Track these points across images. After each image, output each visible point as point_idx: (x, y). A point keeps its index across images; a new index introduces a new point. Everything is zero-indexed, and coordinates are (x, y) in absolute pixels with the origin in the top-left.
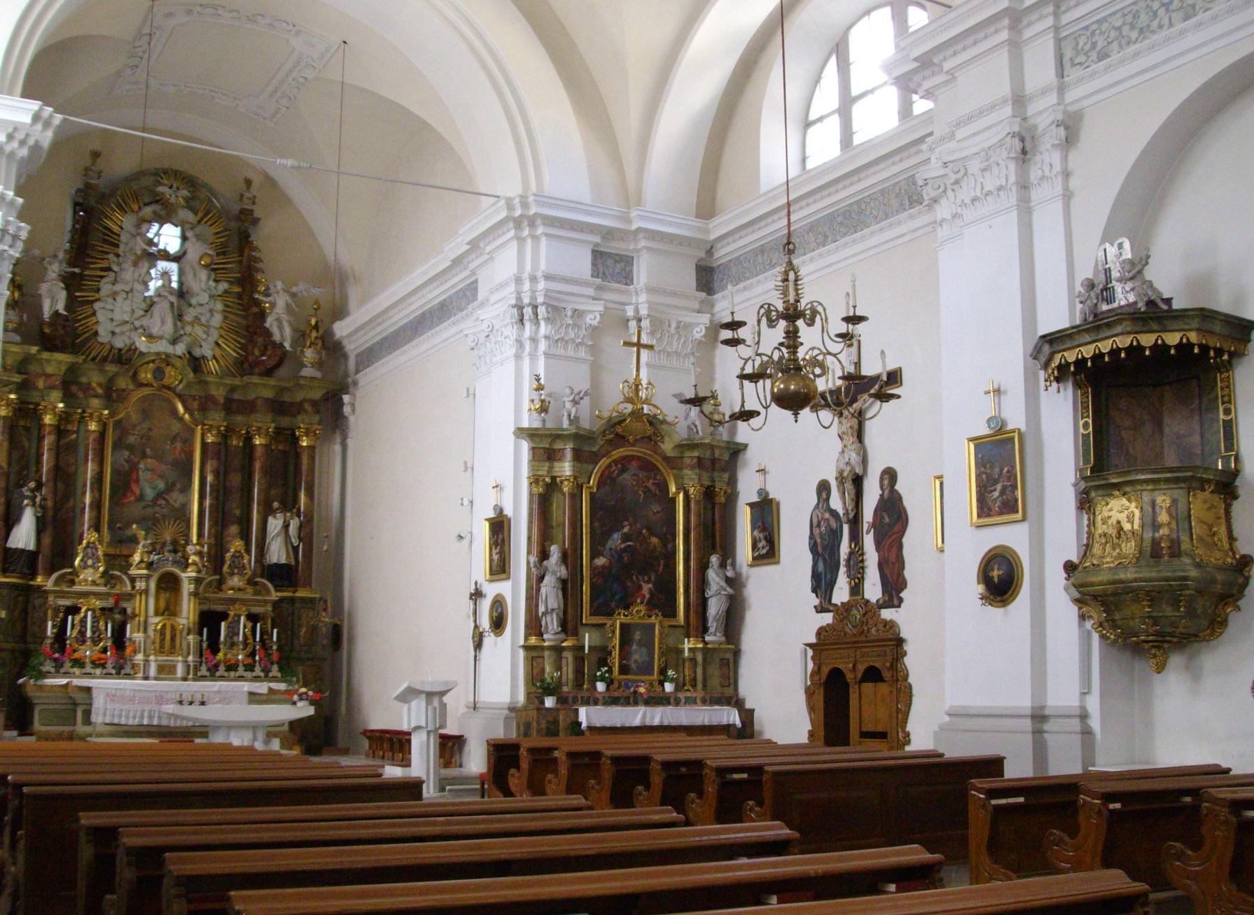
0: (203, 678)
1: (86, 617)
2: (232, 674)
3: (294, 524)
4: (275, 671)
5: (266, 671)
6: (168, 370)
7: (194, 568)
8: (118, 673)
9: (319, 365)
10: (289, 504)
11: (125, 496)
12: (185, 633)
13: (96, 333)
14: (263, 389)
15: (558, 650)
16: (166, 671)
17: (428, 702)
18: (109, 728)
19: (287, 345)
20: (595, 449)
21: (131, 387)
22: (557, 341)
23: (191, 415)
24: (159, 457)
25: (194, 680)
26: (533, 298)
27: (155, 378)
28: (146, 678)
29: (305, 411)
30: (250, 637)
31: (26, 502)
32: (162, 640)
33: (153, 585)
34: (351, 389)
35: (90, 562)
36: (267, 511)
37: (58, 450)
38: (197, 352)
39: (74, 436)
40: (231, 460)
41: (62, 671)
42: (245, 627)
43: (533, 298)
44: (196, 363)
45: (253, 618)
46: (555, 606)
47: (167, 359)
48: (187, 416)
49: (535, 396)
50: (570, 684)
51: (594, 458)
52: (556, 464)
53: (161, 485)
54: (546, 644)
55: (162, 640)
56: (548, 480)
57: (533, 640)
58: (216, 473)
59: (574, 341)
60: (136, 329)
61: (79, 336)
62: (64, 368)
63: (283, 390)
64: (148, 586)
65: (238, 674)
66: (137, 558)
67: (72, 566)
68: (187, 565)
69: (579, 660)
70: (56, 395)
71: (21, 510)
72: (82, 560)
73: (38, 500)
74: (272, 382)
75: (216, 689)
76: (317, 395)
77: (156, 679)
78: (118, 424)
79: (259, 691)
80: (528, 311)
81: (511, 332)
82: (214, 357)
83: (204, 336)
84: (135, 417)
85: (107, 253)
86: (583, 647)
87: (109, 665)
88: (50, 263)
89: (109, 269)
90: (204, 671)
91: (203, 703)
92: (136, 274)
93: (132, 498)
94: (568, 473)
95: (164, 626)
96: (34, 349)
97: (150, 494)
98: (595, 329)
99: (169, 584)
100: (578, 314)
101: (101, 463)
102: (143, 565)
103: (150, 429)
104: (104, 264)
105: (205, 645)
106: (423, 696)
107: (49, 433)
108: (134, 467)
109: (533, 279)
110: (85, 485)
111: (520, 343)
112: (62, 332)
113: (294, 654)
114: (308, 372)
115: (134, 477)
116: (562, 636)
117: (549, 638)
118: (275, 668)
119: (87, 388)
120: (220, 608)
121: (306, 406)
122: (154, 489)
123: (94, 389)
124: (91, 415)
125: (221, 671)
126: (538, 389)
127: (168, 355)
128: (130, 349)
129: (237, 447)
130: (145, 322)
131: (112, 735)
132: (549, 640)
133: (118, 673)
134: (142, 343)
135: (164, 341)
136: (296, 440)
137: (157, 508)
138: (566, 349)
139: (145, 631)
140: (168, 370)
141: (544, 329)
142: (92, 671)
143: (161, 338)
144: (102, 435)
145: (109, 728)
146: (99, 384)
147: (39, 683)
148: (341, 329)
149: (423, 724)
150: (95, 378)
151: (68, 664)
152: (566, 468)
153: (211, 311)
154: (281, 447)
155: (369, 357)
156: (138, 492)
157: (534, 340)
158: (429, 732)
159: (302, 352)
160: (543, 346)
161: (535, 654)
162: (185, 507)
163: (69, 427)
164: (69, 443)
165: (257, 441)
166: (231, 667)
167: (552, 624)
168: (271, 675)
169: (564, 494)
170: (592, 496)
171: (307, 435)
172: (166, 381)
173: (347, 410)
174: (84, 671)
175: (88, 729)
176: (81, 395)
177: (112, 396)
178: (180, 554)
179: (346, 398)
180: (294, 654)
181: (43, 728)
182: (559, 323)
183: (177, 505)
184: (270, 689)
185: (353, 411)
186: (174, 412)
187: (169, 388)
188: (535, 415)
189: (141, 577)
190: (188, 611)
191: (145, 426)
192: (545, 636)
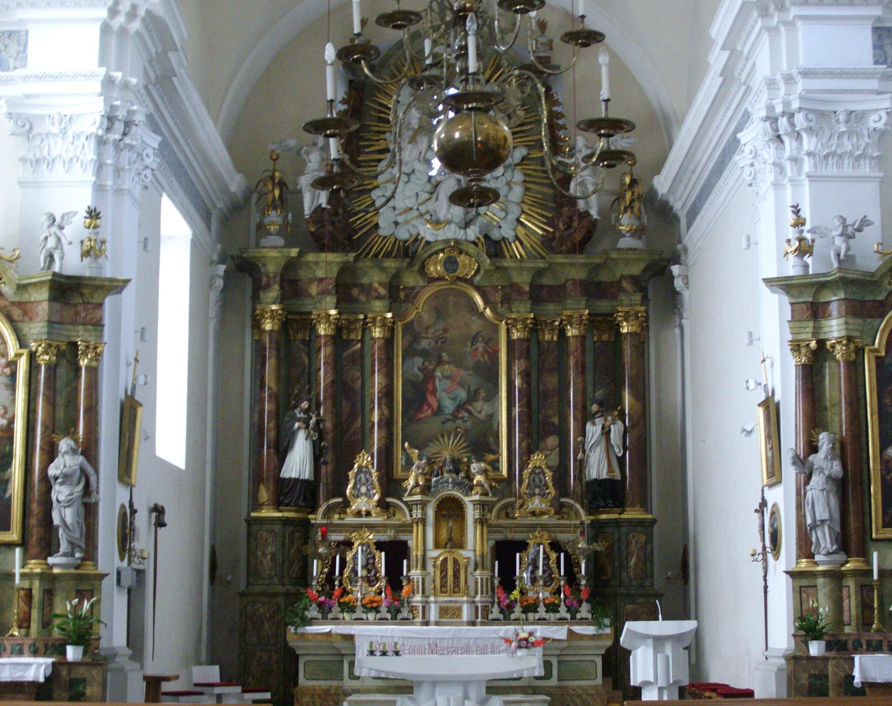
0: (496, 621)
1: (357, 553)
2: (531, 616)
3: (616, 430)
4: (585, 611)
5: (573, 611)
6: (462, 259)
7: (479, 489)
8: (394, 618)
9: (638, 232)
10: (611, 405)
11: (419, 410)
12: (471, 568)
13: (377, 226)
14: (572, 268)
15: (836, 576)
16: (449, 614)
17: (657, 650)
18: (379, 683)
19: (594, 213)
20: (881, 297)
21: (421, 283)
22: (826, 156)
23: (493, 310)
24: (458, 362)
25: (483, 624)
26: (787, 104)
27: (447, 270)
28: (427, 623)
29: (625, 291)
30: (555, 570)
31: (297, 425)
32: (444, 577)
33: (431, 512)
34: (683, 258)
35: (363, 489)
36: (585, 418)
37: (337, 364)
38: (495, 235)
39: (359, 345)
40: (540, 357)
41: (330, 616)
42: (547, 558)
43: (787, 104)
44: (495, 248)
45: (556, 546)
46: (826, 516)
47: (457, 246)
48: (488, 311)
49: (792, 233)
50: (853, 623)
51: (879, 310)
52: (824, 322)
53: (462, 394)
54: (820, 568)
55: (444, 577)
56: (813, 344)
57: (804, 565)
58: (526, 375)
59: (851, 154)
60: (421, 215)
61: (356, 232)
62: (336, 269)
63: (597, 267)
64: (424, 514)
65: (537, 616)
66: (411, 481)
67: (343, 495)
68: (471, 488)
69: (865, 589)
70: (331, 300)
71: (293, 435)
72: (354, 487)
73: (312, 422)
74: (580, 259)
75: (502, 634)
76: (636, 270)
77: (437, 624)
78: (408, 328)
79: (556, 636)
80: (783, 122)
81: (769, 153)
82: (517, 238)
83: (503, 214)
85: (384, 133)
86: (872, 571)
87: (383, 609)
88: (308, 153)
89: (386, 150)
90: (495, 613)
91: (397, 653)
92: (415, 154)
93: (429, 412)
94: (836, 334)
95: (446, 559)
96: (294, 252)
97: (449, 406)
98: (883, 133)
99: (451, 510)
100: (855, 117)
101: (389, 375)
102: (418, 490)
103: (446, 330)
104: (382, 145)
105: (496, 582)
106: (650, 641)
107: (325, 345)
108: (429, 376)
109: (789, 79)
110: (373, 401)
111: (779, 167)
112: (330, 228)
113: (622, 590)
114: (626, 242)
115: (430, 387)
116: (841, 557)
117: (822, 562)
118: (585, 607)
119: (367, 290)
120: (519, 537)
121: (625, 284)
122: (454, 399)
123: (376, 290)
124: (374, 319)
125: (517, 612)
126: (795, 225)
127: (457, 242)
128: (416, 239)
129: (550, 342)
130: (430, 206)
131: (380, 690)
132: (823, 563)
133: (394, 618)
134: (427, 232)
135: (453, 226)
136: (618, 326)
137: (459, 422)
138: (840, 166)
139: (424, 567)
140: (462, 259)
141: (808, 143)
142: (364, 616)
143: (449, 222)
144: (389, 342)
145: (379, 683)
146: (381, 284)
147: (300, 630)
148: (662, 184)
149: (652, 679)
150: (375, 278)
151: (336, 609)
152: (835, 328)
153: (508, 184)
154: (605, 337)
155: (693, 214)
156: (435, 405)
157: (795, 160)
158: (661, 690)
159: (618, 220)
160: (807, 165)
161: (805, 582)
162: (492, 417)
163: (353, 336)
164: (354, 352)
165: (571, 332)
166: (530, 608)
167: (824, 539)
168: (578, 616)
169: (838, 362)
170: (880, 363)
171: (626, 319)
172: (460, 273)
173: (678, 284)
174: (354, 616)
175: (355, 684)
176: (363, 298)
177: (397, 295)
178: (462, 474)
179: (675, 269)
180: (622, 590)
181: (310, 683)
182: (828, 133)
183: (482, 416)
184: (570, 632)
185: (687, 284)
186: (473, 307)
187: (463, 279)
188: (791, 257)
189: (416, 503)
190: (475, 542)
191: (440, 326)
192: (818, 558)
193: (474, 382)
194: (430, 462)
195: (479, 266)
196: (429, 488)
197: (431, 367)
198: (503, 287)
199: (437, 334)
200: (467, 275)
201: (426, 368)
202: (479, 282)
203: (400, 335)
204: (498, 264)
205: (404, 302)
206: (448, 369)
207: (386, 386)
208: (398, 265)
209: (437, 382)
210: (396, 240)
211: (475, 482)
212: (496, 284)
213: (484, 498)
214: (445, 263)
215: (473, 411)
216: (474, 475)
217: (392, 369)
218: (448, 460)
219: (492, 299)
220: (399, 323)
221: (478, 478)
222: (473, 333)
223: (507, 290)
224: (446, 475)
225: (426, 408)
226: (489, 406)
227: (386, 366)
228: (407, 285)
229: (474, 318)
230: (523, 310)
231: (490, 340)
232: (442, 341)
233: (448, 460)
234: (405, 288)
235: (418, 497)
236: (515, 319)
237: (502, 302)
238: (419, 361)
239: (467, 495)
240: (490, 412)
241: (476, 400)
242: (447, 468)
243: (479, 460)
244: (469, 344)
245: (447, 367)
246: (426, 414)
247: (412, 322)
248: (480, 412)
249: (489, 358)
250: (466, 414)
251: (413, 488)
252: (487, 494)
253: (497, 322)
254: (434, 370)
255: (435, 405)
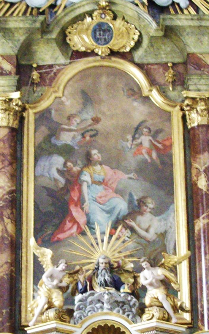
11: (59, 227)
21: (62, 60)
23: (163, 92)
24: (114, 161)
27: (97, 40)
53: (122, 206)
84: (71, 104)
102: (51, 313)
103: (96, 120)
108: (73, 181)
115: (75, 196)
122: (109, 212)
172: (116, 44)
178: (125, 289)
183: (151, 236)
186: (134, 91)
191: (88, 115)
193: (138, 188)
194: (73, 273)
195: (140, 36)
196: (70, 312)
197: (76, 169)
198: (174, 64)
199: (83, 126)
200: (124, 46)
201: (69, 171)
202: (140, 58)
203: (32, 127)
204: (168, 23)
205: (38, 85)
206: (100, 171)
207: (10, 192)
208: (27, 26)
209: (85, 188)
210: (28, 6)
211: (147, 301)
212: (165, 60)
213: (165, 325)
214: (94, 31)
215: (137, 228)
216: (144, 289)
217: (21, 171)
218: (102, 266)
219: (161, 80)
220: (31, 112)
221: (155, 294)
222: (136, 124)
223: (181, 69)
224: (99, 290)
225: (68, 224)
226: (160, 220)
227: (11, 164)
228: (41, 64)
229: (135, 104)
230: (205, 87)
231: (158, 132)
232: (91, 134)
233: (102, 266)
234: (39, 67)
235: (53, 324)
236: (194, 99)
237: (174, 83)
238: (58, 161)
239: (135, 322)
240: (162, 230)
241: (141, 214)
242: (100, 279)
243: (154, 263)
244: (129, 137)
245: (98, 168)
246: (67, 234)
247: (48, 110)
248: (147, 231)
249: (158, 156)
250: (128, 233)
251: (42, 313)
252: (169, 319)
253: (168, 109)
254: (80, 173)
255: (82, 220)
